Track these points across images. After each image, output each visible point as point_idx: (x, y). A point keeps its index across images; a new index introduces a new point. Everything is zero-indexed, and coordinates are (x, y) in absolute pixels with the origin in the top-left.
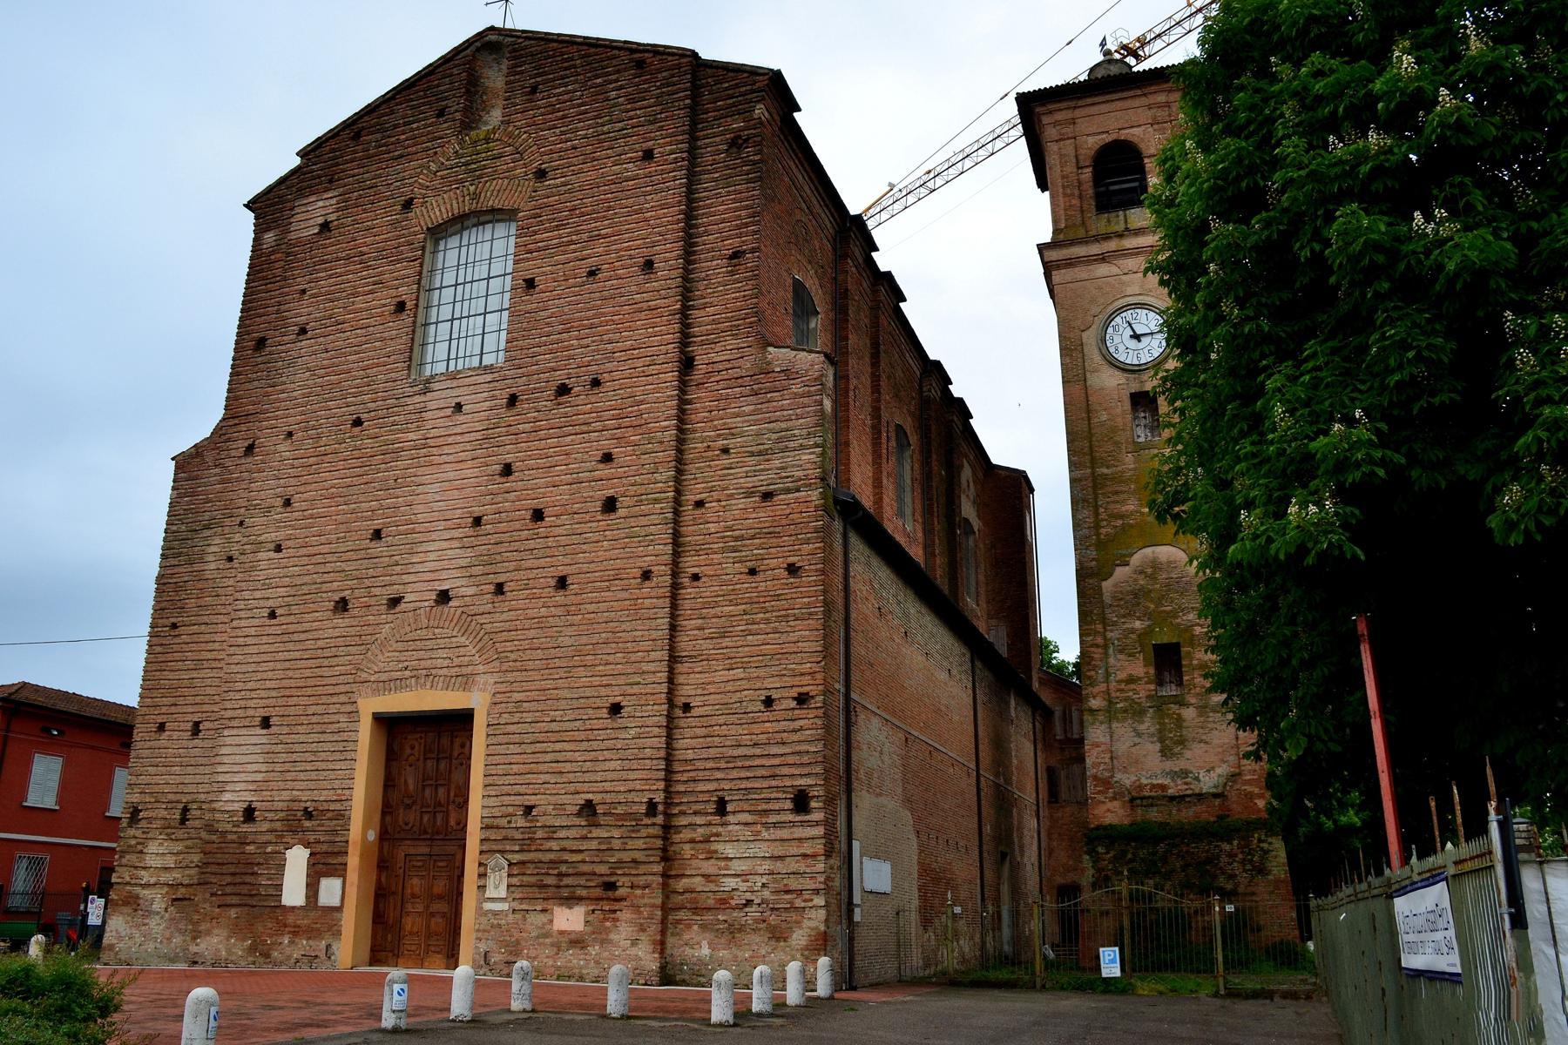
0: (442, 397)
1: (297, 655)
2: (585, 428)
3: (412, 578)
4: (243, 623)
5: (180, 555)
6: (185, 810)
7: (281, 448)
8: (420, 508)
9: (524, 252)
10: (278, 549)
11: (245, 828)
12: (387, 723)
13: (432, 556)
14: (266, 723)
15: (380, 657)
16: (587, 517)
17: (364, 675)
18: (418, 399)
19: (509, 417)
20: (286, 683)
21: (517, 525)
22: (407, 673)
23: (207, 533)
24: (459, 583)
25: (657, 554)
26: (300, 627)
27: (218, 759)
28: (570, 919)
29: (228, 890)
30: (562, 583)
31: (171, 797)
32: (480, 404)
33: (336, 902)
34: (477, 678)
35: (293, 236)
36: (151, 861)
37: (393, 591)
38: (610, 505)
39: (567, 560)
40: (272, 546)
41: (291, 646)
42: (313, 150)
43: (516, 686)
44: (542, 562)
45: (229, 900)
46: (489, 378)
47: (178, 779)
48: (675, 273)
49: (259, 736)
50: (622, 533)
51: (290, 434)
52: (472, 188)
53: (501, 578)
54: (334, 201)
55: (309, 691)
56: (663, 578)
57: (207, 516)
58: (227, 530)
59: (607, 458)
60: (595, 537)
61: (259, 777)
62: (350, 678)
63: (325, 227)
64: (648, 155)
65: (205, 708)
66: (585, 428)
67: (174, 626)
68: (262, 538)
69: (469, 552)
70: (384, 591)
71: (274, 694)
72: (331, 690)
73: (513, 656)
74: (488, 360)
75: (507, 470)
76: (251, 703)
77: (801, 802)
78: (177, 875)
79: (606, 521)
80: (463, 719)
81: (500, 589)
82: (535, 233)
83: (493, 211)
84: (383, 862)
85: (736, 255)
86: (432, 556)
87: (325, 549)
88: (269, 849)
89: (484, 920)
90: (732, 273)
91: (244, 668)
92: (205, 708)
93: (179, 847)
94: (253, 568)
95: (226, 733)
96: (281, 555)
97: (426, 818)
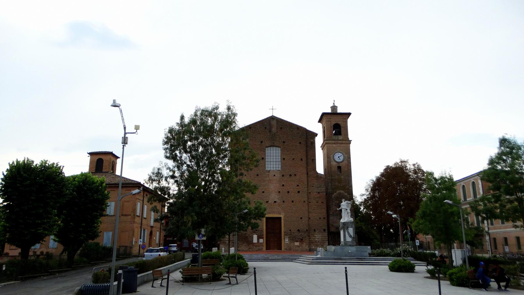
0: (272, 174)
9: (282, 154)
19: (283, 178)
25: (306, 199)
28: (297, 244)
30: (293, 202)
32: (278, 176)
37: (267, 200)
38: (299, 192)
56: (306, 202)
59: (298, 186)
74: (278, 169)
75: (283, 185)
77: (324, 230)
79: (298, 194)
80: (281, 218)
81: (284, 202)
84: (267, 237)
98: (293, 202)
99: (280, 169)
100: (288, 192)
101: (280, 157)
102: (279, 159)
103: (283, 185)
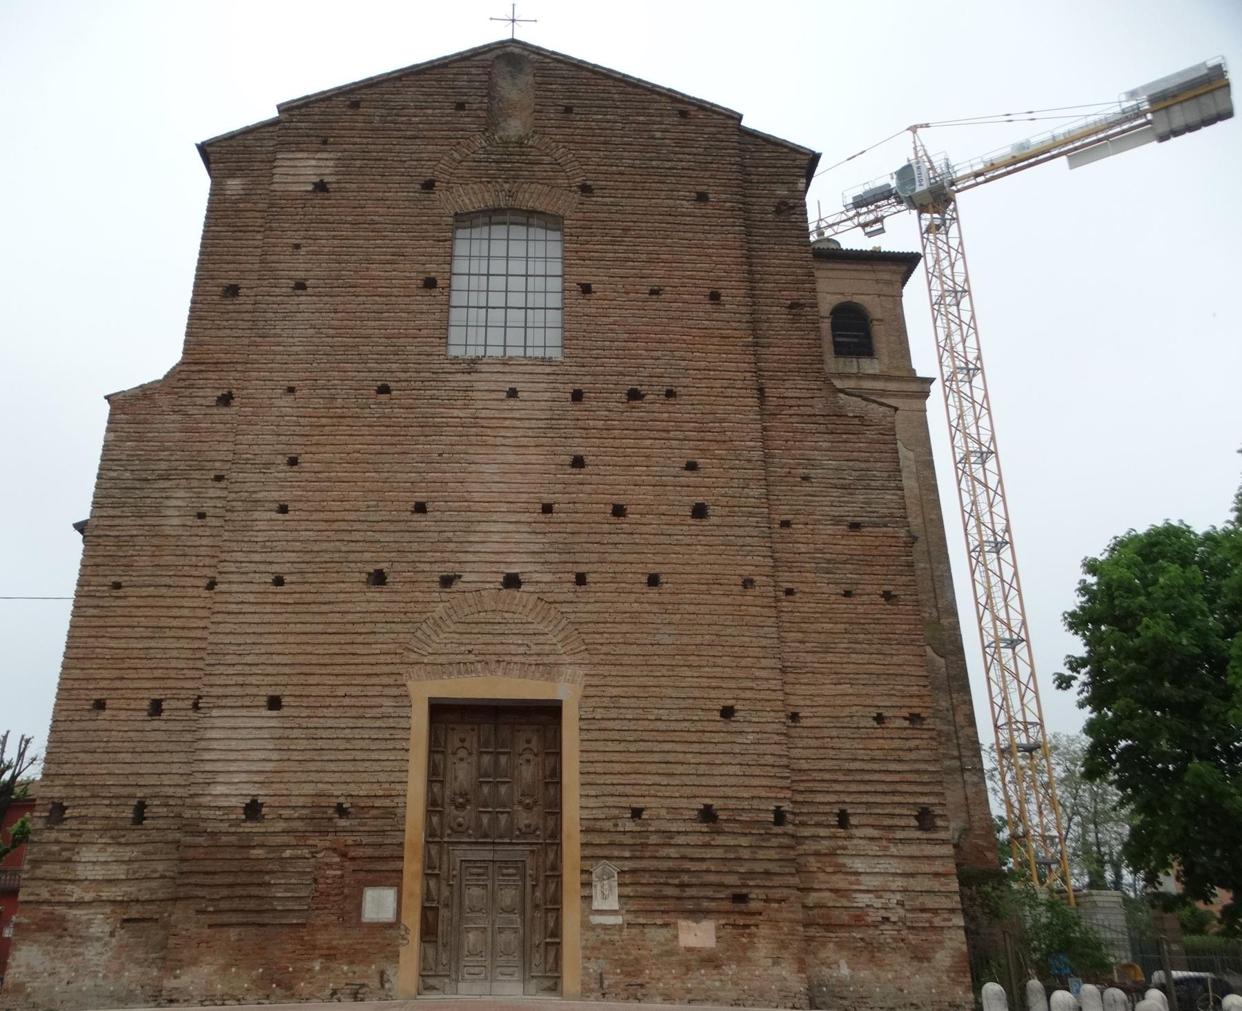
1: (320, 628)
2: (665, 435)
3: (470, 557)
4: (235, 588)
5: (124, 505)
6: (141, 807)
7: (276, 402)
8: (477, 487)
10: (283, 509)
11: (249, 827)
12: (443, 713)
13: (496, 537)
14: (275, 703)
15: (434, 637)
16: (677, 520)
17: (413, 657)
18: (459, 377)
19: (574, 410)
20: (301, 659)
21: (597, 518)
22: (471, 657)
23: (162, 484)
24: (531, 568)
25: (754, 563)
26: (321, 598)
27: (203, 744)
29: (224, 905)
31: (115, 790)
32: (539, 396)
33: (388, 915)
34: (563, 668)
35: (275, 187)
36: (82, 871)
37: (448, 569)
38: (700, 511)
39: (659, 558)
40: (275, 506)
41: (308, 618)
42: (299, 107)
43: (608, 681)
44: (630, 558)
45: (225, 918)
46: (548, 370)
47: (128, 769)
48: (744, 309)
49: (270, 719)
50: (717, 541)
51: (291, 390)
52: (507, 186)
53: (582, 569)
54: (331, 163)
55: (338, 670)
57: (163, 465)
58: (195, 483)
59: (692, 466)
60: (688, 540)
61: (269, 766)
62: (397, 659)
63: (321, 187)
64: (702, 197)
65: (170, 683)
66: (665, 435)
67: (117, 586)
68: (259, 496)
69: (540, 538)
70: (435, 567)
71: (287, 670)
72: (369, 670)
73: (604, 649)
76: (253, 680)
78: (130, 889)
80: (552, 711)
81: (581, 579)
82: (587, 242)
83: (532, 213)
85: (791, 307)
86: (496, 537)
87: (352, 516)
88: (288, 853)
89: (589, 934)
90: (793, 321)
91: (240, 639)
92: (170, 683)
93: (128, 853)
94: (246, 529)
95: (215, 713)
96: (287, 517)
97: (485, 819)
98: (653, 581)
99: (556, 354)
100: (619, 511)
101: (556, 284)
102: (550, 290)
103: (578, 462)
